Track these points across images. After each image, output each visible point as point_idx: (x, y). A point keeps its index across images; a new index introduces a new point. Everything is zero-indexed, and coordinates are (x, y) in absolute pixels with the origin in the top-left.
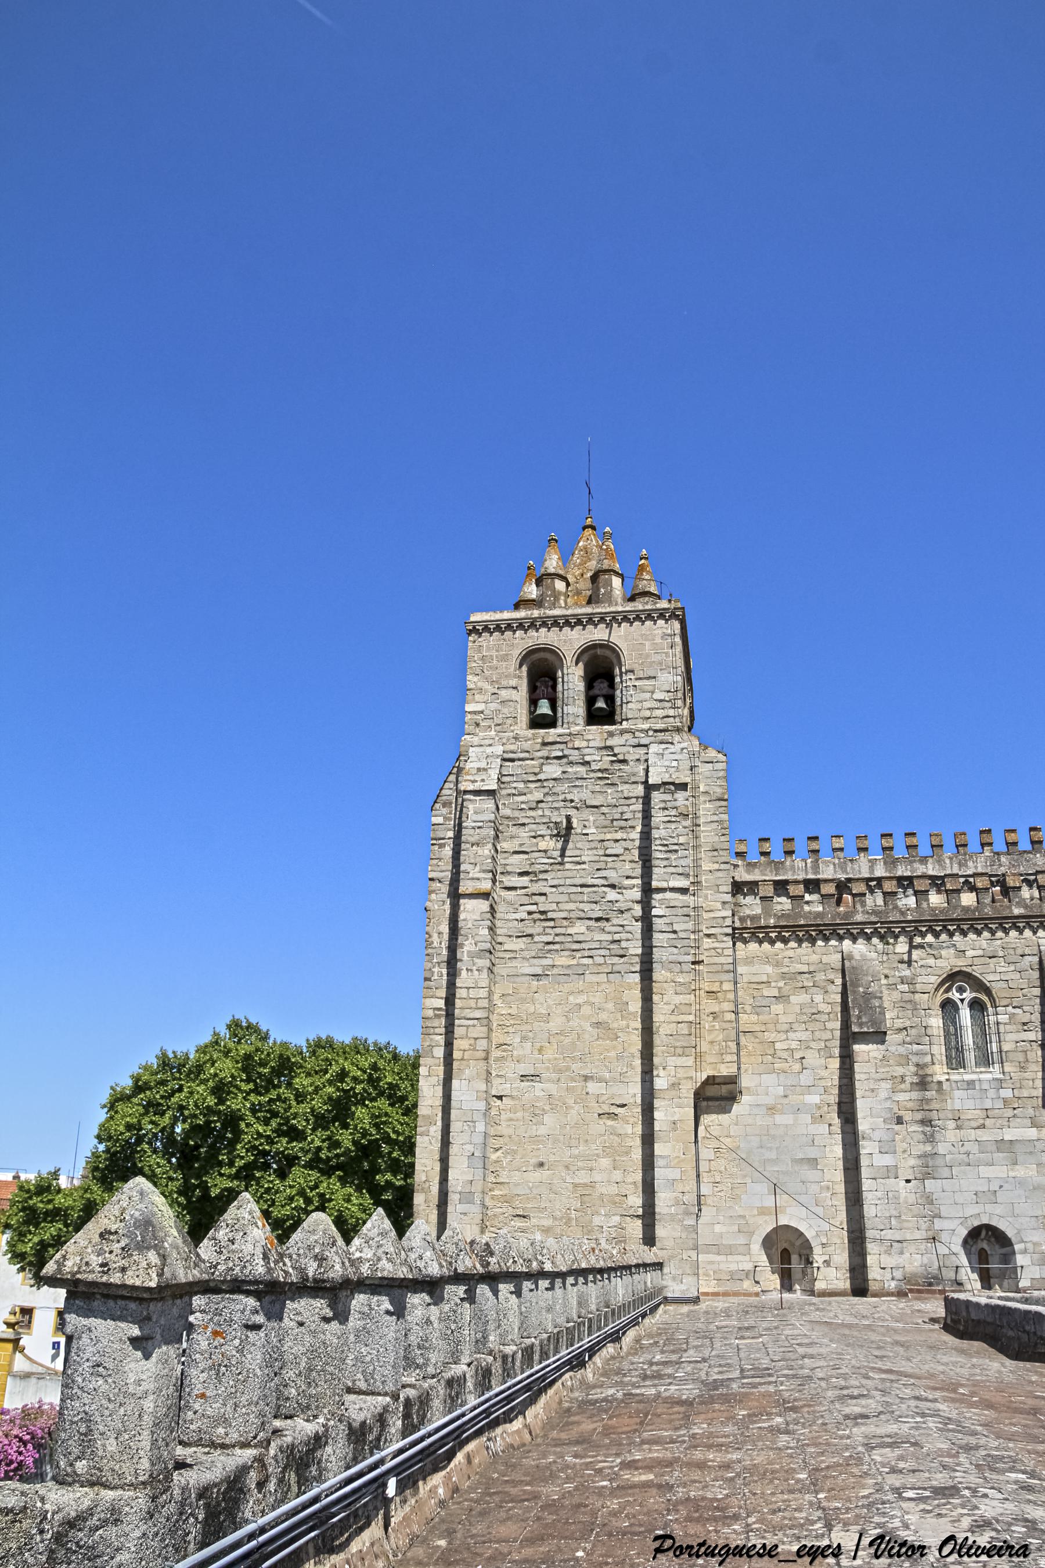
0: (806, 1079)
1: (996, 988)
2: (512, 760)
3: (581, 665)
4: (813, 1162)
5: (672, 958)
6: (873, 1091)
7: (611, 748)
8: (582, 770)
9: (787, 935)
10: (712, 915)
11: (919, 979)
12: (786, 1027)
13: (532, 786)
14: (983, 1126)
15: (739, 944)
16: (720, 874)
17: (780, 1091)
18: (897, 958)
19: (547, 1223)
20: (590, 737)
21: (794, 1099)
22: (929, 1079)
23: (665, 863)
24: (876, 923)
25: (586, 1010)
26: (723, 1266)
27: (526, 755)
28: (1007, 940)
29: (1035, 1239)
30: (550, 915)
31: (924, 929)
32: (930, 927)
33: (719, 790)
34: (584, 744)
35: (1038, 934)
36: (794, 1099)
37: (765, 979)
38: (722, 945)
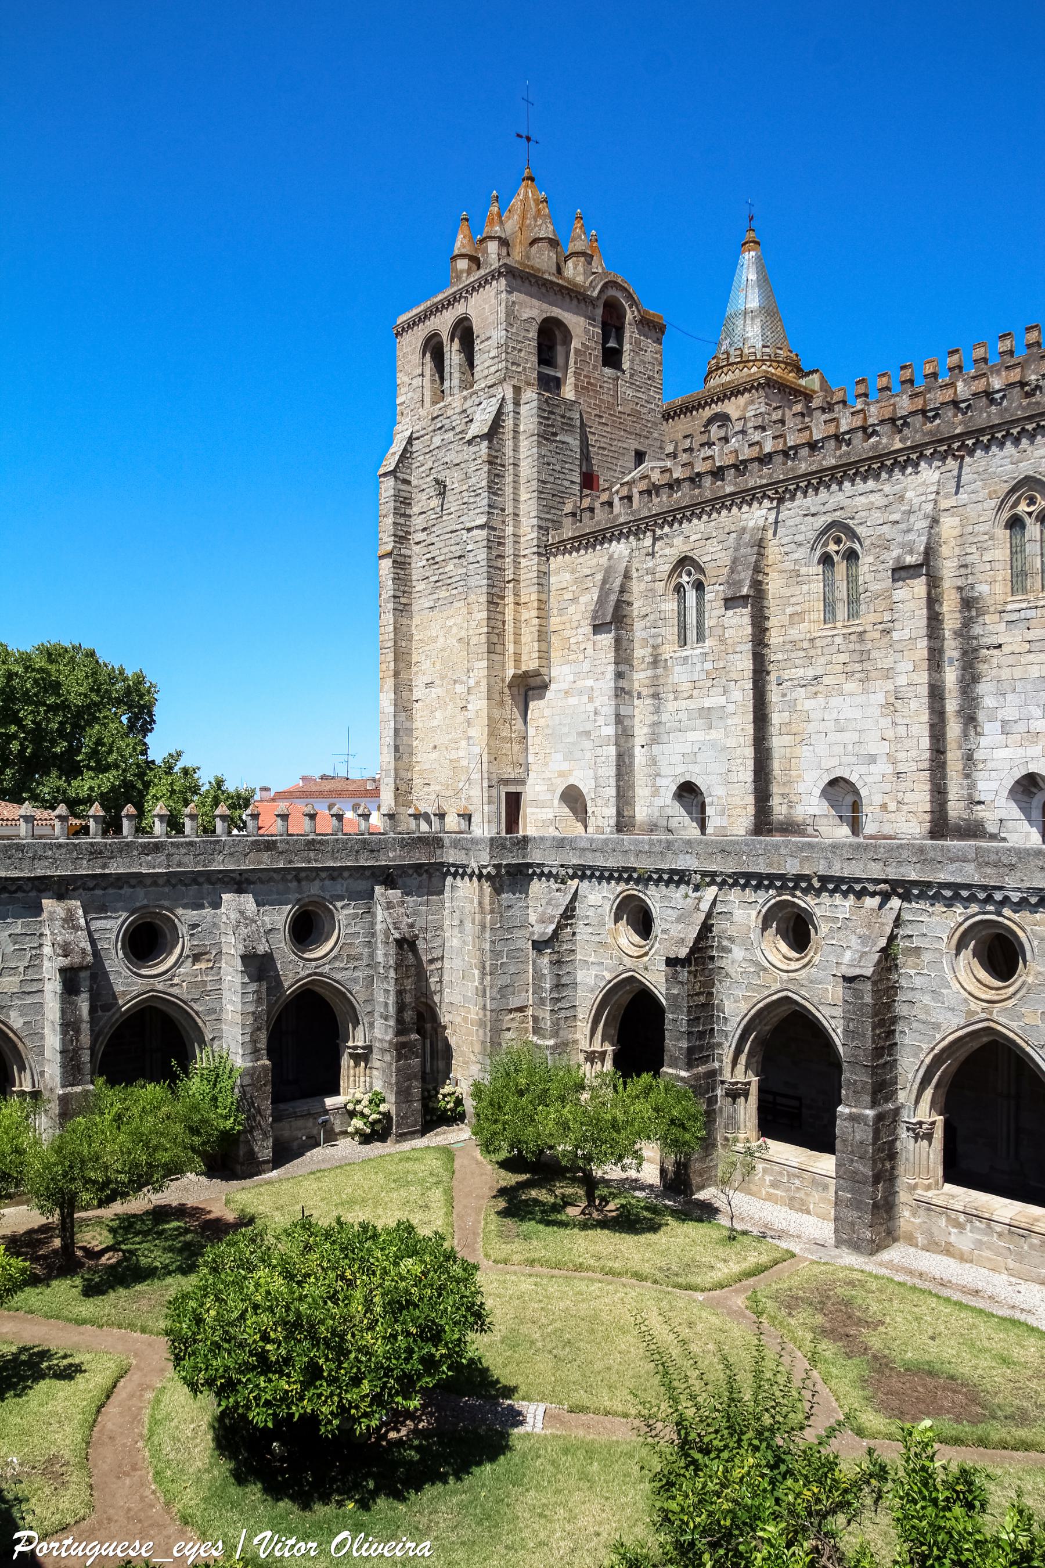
0: (586, 666)
1: (708, 568)
2: (418, 438)
3: (456, 340)
4: (588, 733)
5: (477, 583)
6: (603, 673)
7: (465, 411)
8: (451, 434)
9: (576, 544)
10: (526, 538)
11: (658, 569)
12: (575, 624)
13: (427, 456)
14: (691, 697)
15: (552, 558)
16: (531, 502)
17: (571, 678)
18: (645, 551)
19: (438, 788)
20: (454, 405)
21: (580, 684)
22: (659, 658)
23: (474, 506)
24: (629, 522)
25: (454, 630)
26: (539, 816)
27: (422, 432)
28: (721, 519)
29: (719, 793)
30: (437, 559)
31: (660, 522)
32: (665, 518)
33: (531, 426)
34: (452, 412)
35: (743, 510)
36: (580, 684)
37: (565, 585)
38: (532, 563)
